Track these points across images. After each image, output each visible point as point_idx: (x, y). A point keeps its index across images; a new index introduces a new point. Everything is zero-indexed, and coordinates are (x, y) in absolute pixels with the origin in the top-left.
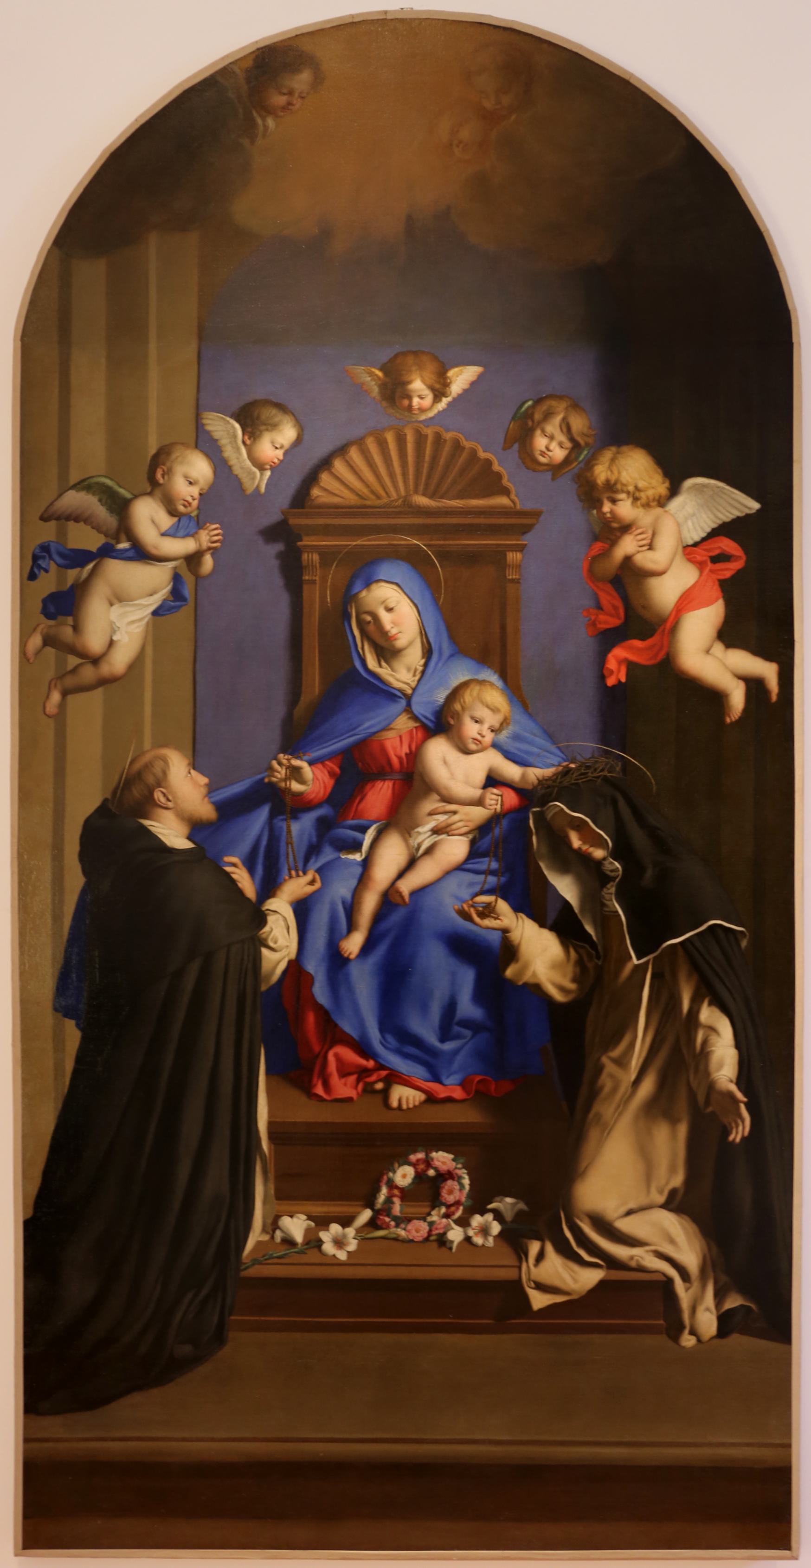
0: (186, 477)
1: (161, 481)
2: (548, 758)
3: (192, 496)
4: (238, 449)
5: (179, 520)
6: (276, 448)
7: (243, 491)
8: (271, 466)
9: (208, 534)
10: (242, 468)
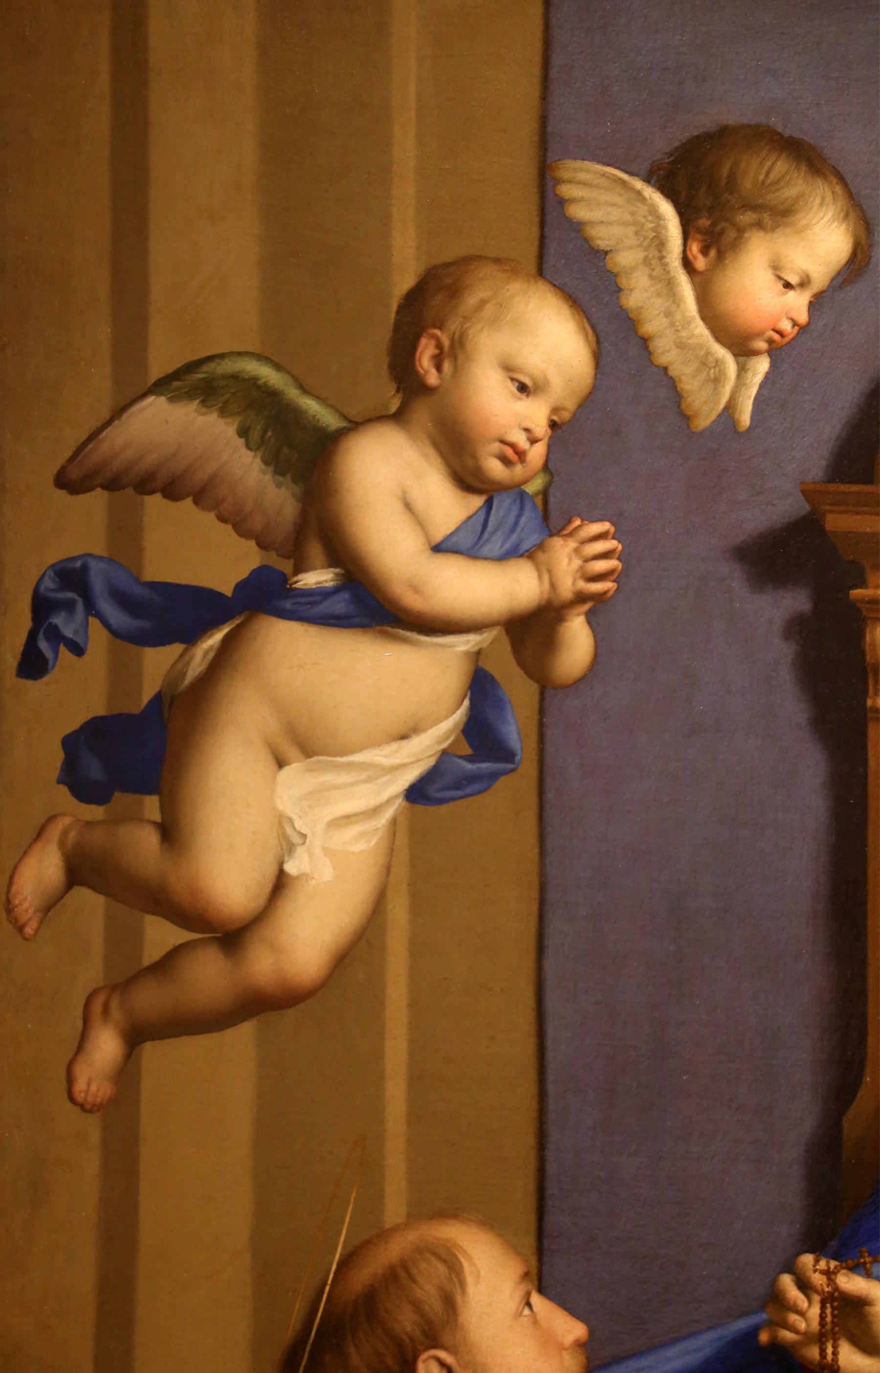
0: (509, 369)
1: (432, 379)
3: (527, 430)
4: (670, 284)
5: (489, 504)
6: (788, 286)
7: (686, 418)
8: (770, 341)
9: (577, 551)
10: (681, 346)
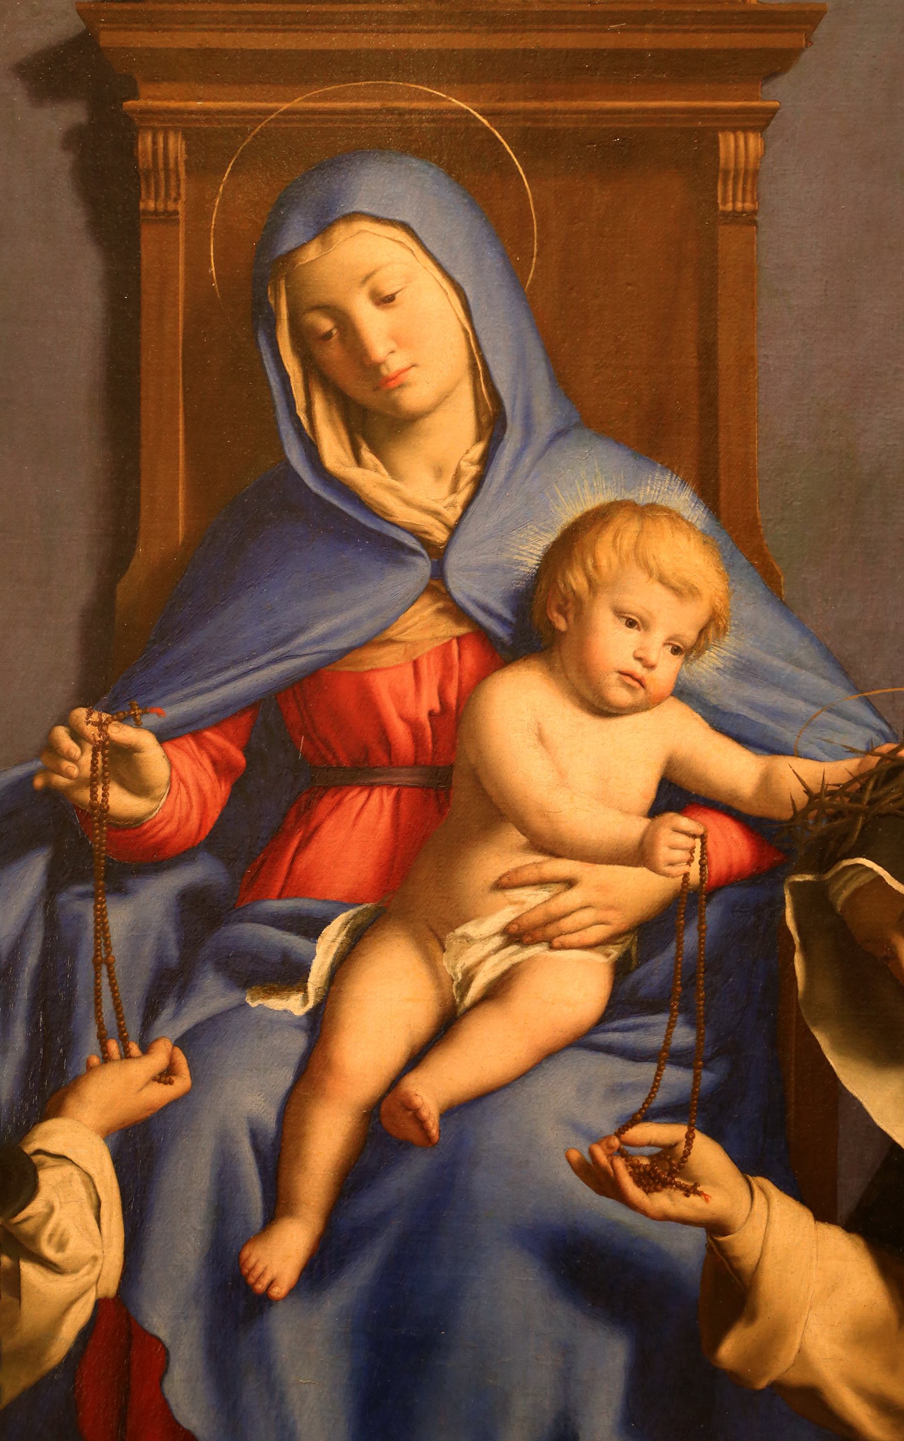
2: (837, 730)
